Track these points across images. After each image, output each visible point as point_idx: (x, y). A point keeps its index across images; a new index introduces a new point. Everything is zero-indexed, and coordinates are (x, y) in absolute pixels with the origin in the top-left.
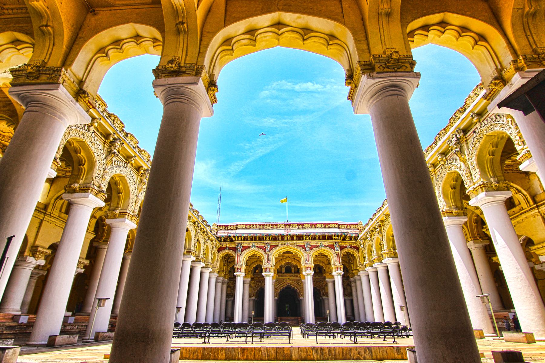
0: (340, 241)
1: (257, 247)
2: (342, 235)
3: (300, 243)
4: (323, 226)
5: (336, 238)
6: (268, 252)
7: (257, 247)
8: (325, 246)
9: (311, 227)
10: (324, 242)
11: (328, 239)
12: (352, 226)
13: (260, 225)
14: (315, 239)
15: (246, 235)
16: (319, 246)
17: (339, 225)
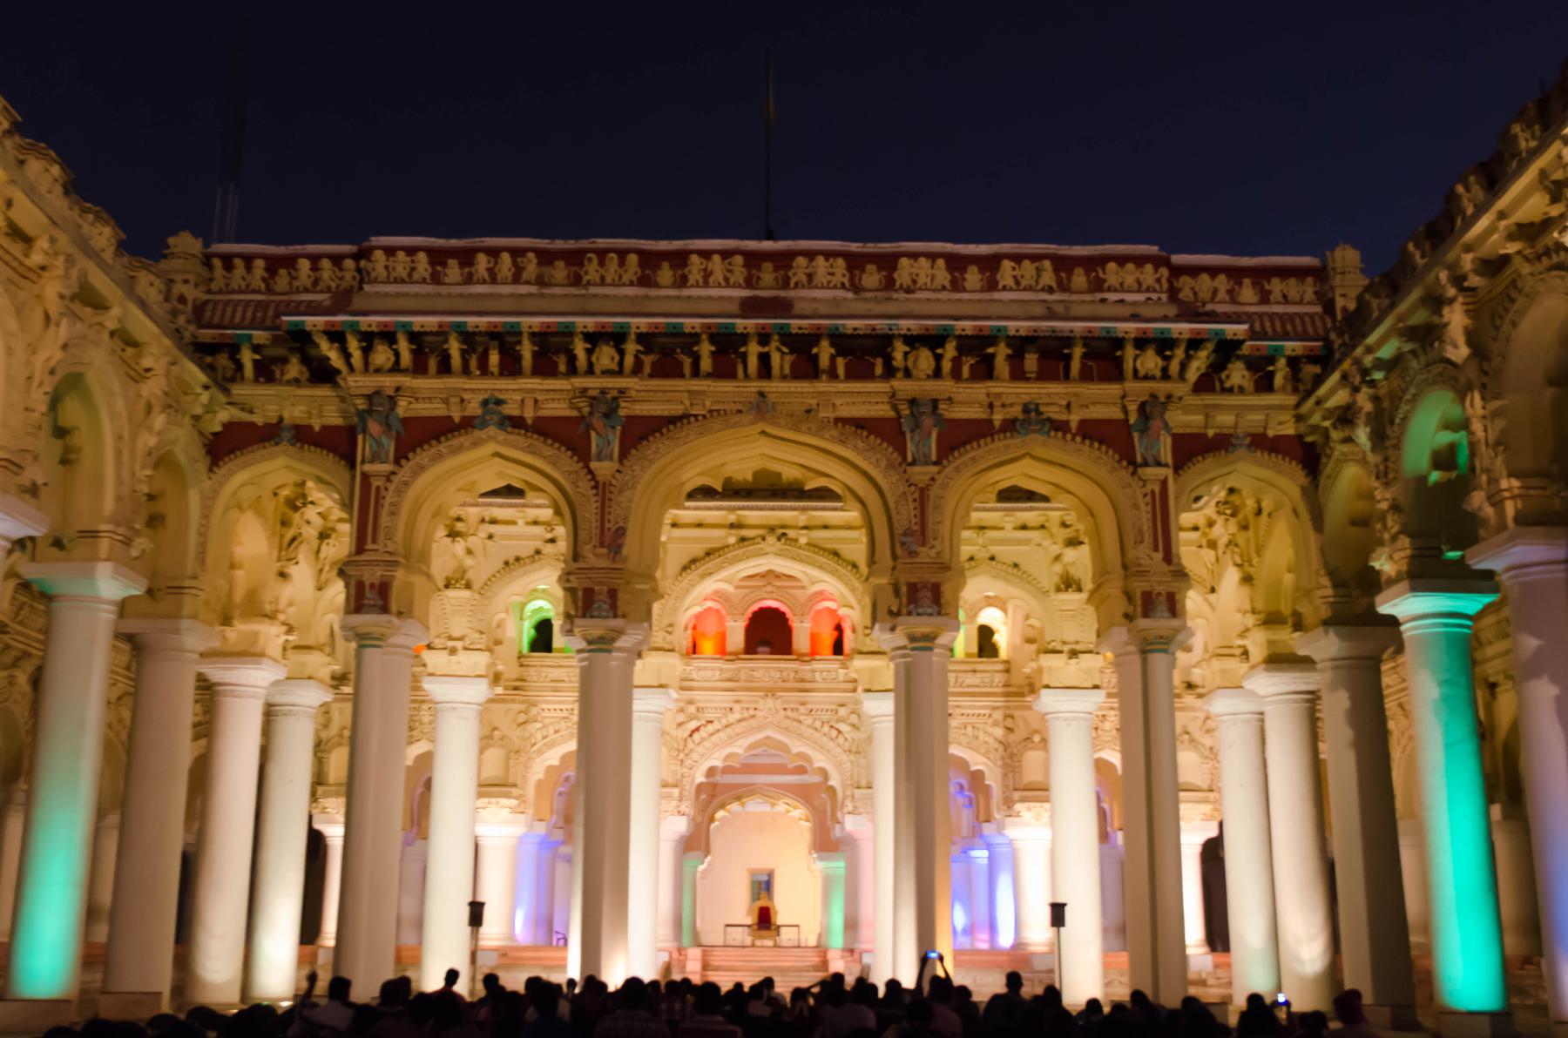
0: (1180, 389)
1: (517, 423)
2: (1194, 344)
3: (868, 398)
4: (1048, 278)
5: (1150, 361)
6: (603, 468)
7: (517, 423)
8: (1060, 427)
9: (956, 286)
10: (1051, 395)
11: (1086, 376)
12: (1276, 286)
13: (546, 257)
14: (985, 371)
15: (430, 322)
16: (1010, 426)
17: (1177, 271)
